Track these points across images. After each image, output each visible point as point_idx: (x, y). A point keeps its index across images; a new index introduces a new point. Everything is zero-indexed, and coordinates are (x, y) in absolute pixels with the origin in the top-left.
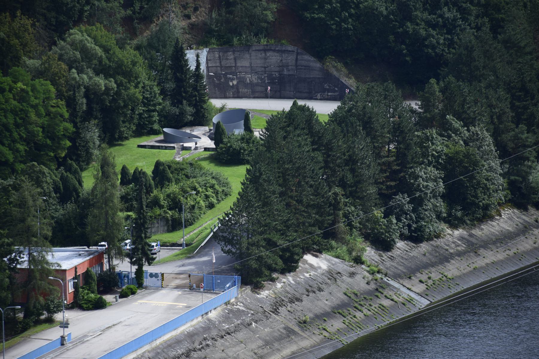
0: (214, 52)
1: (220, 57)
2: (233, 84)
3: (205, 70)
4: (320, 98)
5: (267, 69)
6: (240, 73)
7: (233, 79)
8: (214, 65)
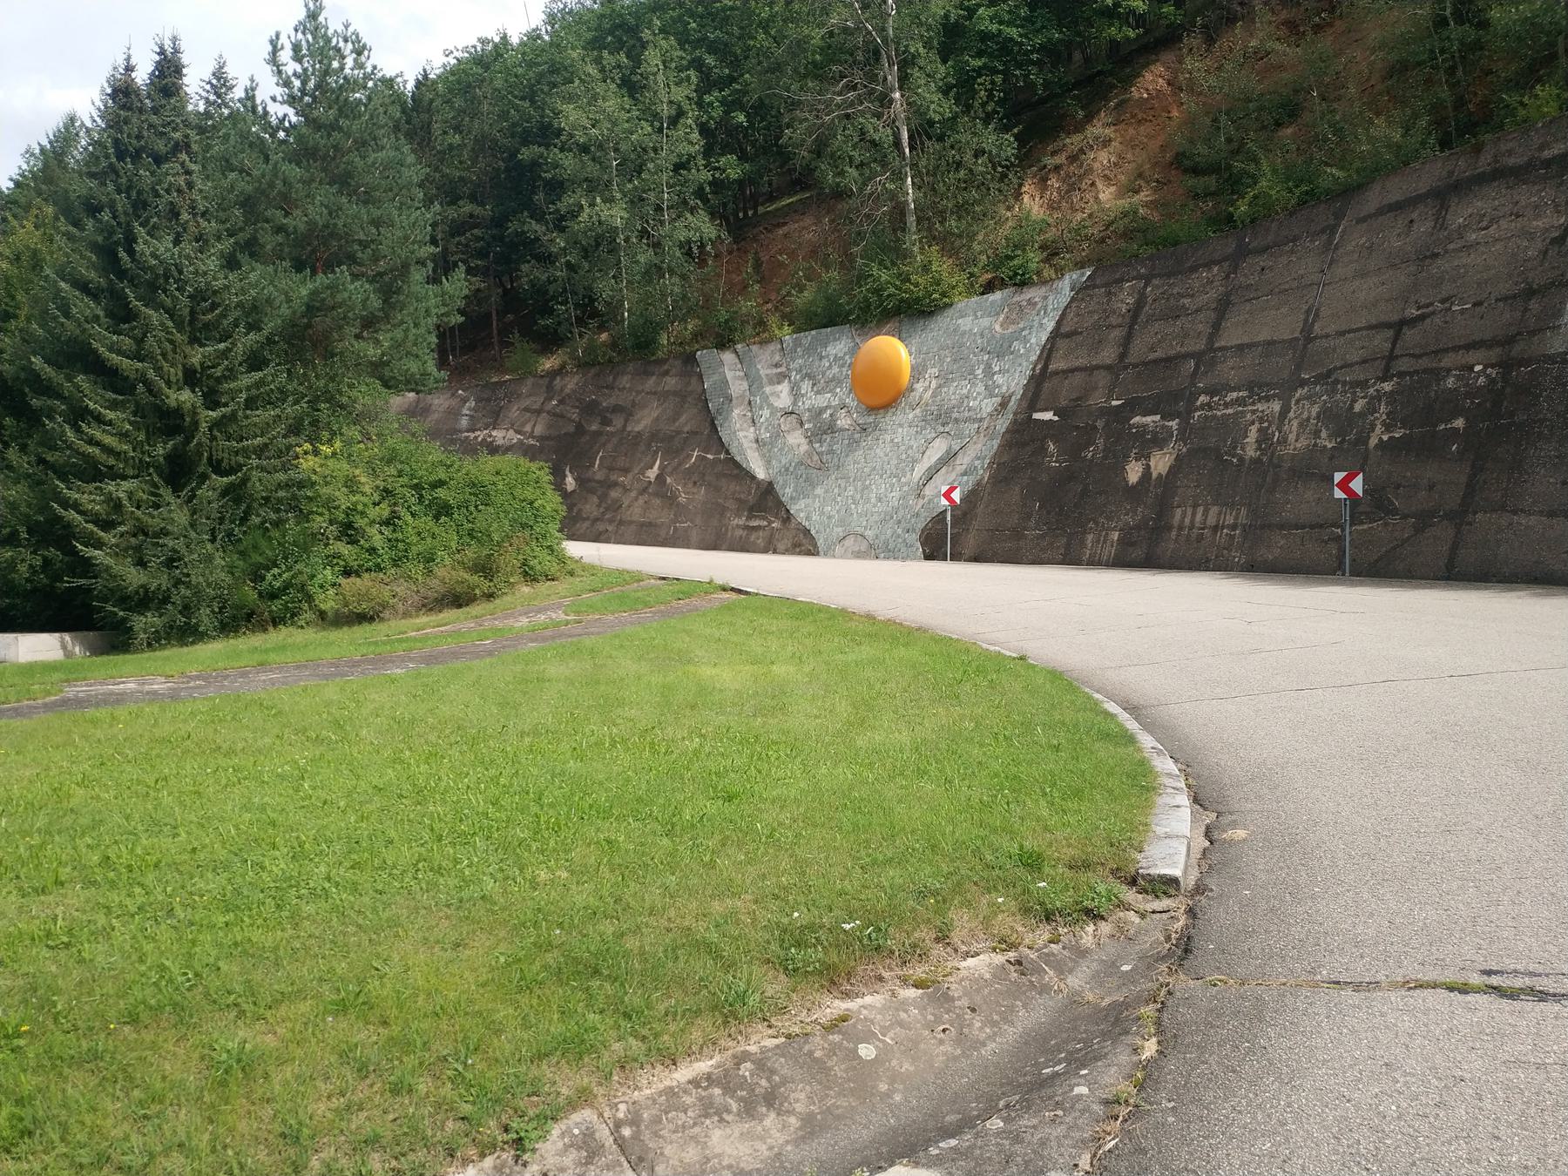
0: (1121, 280)
3: (1013, 404)
5: (1410, 336)
6: (1211, 392)
7: (1157, 440)
8: (1077, 364)
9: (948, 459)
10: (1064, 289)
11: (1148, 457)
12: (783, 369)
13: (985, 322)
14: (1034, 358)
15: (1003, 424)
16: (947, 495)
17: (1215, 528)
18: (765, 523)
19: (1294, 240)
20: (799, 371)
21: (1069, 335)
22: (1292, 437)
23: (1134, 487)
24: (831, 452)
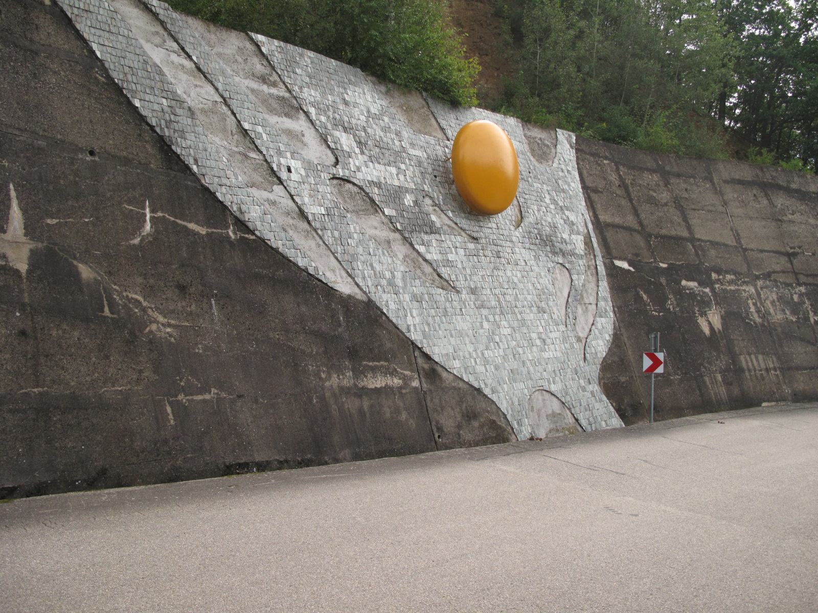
18: (397, 382)
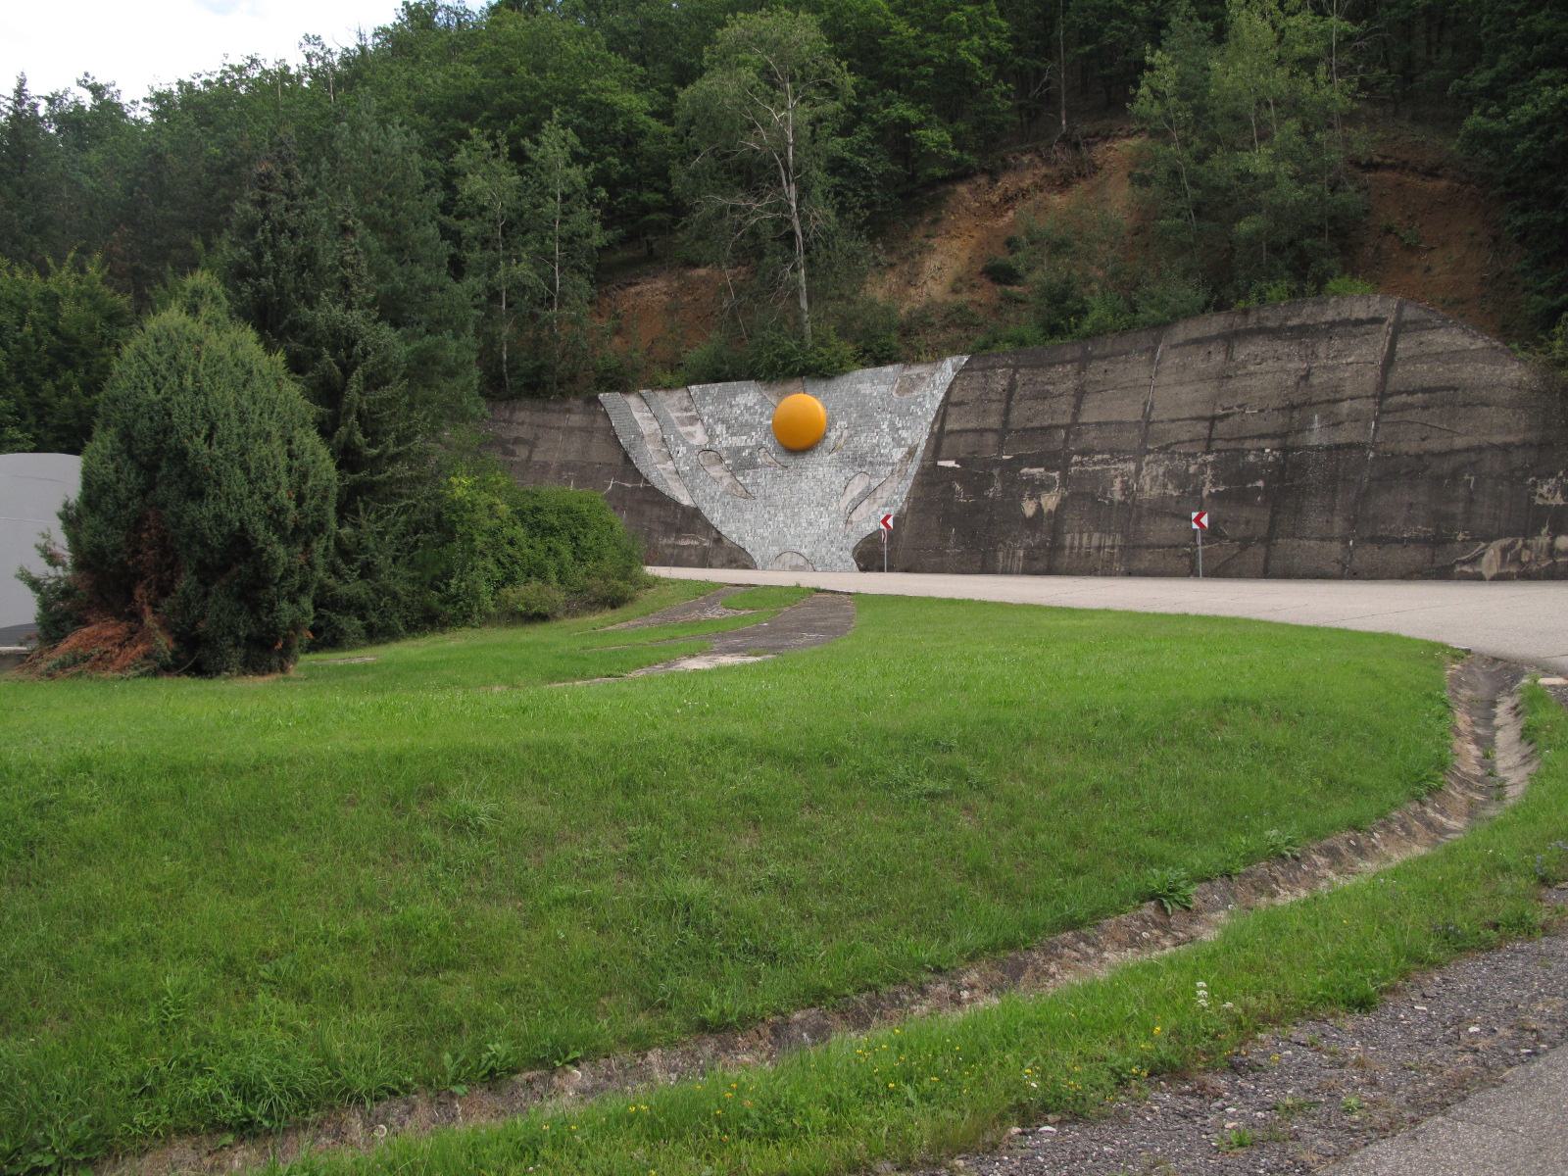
0: (993, 367)
1: (1010, 391)
2: (1039, 507)
3: (919, 453)
4: (1494, 571)
5: (1220, 426)
6: (1083, 453)
7: (1045, 486)
8: (970, 426)
9: (868, 494)
10: (948, 369)
11: (1039, 497)
12: (694, 413)
13: (883, 388)
14: (931, 420)
15: (913, 469)
16: (884, 521)
17: (1099, 548)
19: (1127, 353)
20: (711, 416)
21: (956, 404)
22: (1147, 487)
23: (1031, 519)
24: (756, 484)
